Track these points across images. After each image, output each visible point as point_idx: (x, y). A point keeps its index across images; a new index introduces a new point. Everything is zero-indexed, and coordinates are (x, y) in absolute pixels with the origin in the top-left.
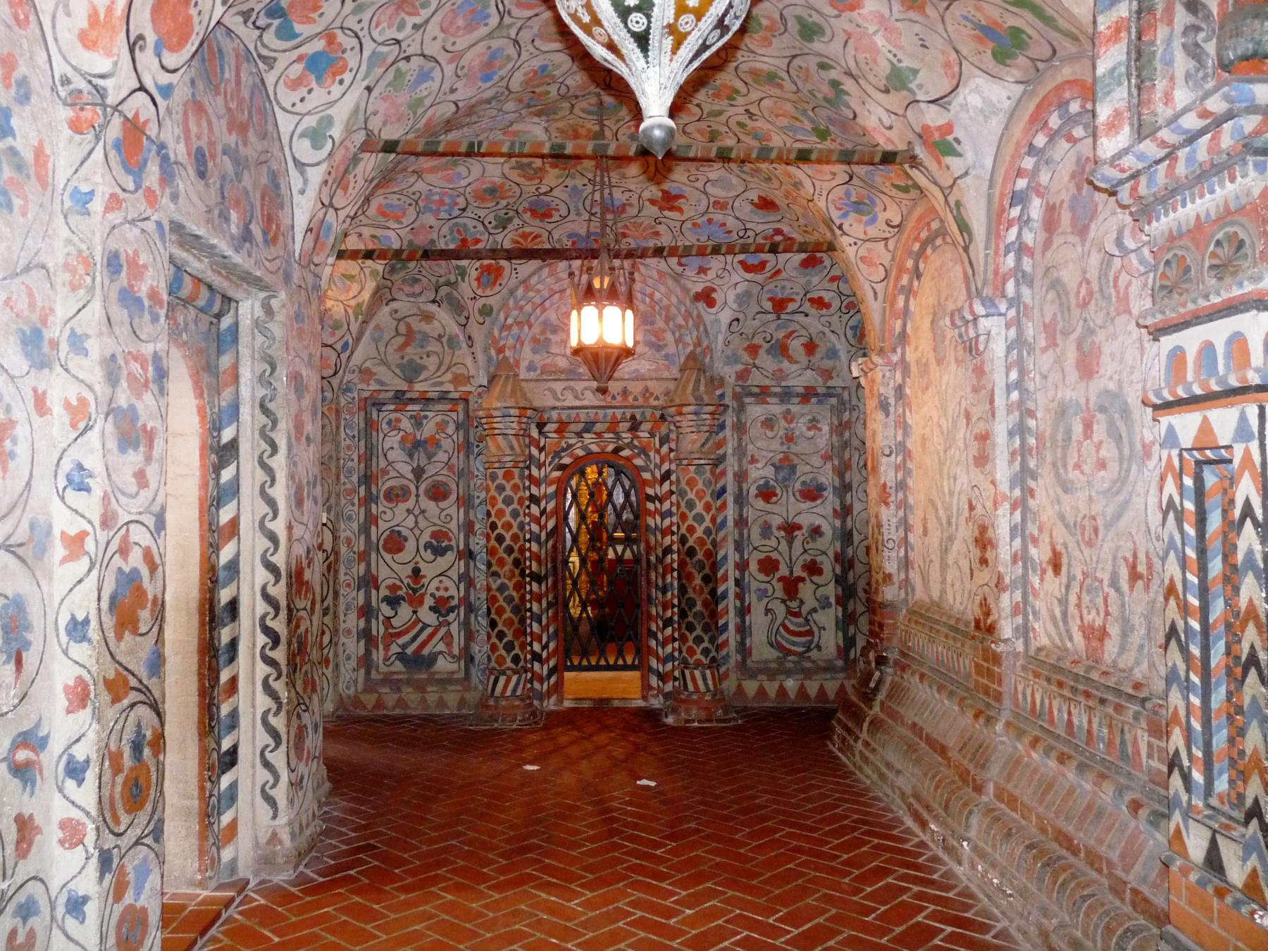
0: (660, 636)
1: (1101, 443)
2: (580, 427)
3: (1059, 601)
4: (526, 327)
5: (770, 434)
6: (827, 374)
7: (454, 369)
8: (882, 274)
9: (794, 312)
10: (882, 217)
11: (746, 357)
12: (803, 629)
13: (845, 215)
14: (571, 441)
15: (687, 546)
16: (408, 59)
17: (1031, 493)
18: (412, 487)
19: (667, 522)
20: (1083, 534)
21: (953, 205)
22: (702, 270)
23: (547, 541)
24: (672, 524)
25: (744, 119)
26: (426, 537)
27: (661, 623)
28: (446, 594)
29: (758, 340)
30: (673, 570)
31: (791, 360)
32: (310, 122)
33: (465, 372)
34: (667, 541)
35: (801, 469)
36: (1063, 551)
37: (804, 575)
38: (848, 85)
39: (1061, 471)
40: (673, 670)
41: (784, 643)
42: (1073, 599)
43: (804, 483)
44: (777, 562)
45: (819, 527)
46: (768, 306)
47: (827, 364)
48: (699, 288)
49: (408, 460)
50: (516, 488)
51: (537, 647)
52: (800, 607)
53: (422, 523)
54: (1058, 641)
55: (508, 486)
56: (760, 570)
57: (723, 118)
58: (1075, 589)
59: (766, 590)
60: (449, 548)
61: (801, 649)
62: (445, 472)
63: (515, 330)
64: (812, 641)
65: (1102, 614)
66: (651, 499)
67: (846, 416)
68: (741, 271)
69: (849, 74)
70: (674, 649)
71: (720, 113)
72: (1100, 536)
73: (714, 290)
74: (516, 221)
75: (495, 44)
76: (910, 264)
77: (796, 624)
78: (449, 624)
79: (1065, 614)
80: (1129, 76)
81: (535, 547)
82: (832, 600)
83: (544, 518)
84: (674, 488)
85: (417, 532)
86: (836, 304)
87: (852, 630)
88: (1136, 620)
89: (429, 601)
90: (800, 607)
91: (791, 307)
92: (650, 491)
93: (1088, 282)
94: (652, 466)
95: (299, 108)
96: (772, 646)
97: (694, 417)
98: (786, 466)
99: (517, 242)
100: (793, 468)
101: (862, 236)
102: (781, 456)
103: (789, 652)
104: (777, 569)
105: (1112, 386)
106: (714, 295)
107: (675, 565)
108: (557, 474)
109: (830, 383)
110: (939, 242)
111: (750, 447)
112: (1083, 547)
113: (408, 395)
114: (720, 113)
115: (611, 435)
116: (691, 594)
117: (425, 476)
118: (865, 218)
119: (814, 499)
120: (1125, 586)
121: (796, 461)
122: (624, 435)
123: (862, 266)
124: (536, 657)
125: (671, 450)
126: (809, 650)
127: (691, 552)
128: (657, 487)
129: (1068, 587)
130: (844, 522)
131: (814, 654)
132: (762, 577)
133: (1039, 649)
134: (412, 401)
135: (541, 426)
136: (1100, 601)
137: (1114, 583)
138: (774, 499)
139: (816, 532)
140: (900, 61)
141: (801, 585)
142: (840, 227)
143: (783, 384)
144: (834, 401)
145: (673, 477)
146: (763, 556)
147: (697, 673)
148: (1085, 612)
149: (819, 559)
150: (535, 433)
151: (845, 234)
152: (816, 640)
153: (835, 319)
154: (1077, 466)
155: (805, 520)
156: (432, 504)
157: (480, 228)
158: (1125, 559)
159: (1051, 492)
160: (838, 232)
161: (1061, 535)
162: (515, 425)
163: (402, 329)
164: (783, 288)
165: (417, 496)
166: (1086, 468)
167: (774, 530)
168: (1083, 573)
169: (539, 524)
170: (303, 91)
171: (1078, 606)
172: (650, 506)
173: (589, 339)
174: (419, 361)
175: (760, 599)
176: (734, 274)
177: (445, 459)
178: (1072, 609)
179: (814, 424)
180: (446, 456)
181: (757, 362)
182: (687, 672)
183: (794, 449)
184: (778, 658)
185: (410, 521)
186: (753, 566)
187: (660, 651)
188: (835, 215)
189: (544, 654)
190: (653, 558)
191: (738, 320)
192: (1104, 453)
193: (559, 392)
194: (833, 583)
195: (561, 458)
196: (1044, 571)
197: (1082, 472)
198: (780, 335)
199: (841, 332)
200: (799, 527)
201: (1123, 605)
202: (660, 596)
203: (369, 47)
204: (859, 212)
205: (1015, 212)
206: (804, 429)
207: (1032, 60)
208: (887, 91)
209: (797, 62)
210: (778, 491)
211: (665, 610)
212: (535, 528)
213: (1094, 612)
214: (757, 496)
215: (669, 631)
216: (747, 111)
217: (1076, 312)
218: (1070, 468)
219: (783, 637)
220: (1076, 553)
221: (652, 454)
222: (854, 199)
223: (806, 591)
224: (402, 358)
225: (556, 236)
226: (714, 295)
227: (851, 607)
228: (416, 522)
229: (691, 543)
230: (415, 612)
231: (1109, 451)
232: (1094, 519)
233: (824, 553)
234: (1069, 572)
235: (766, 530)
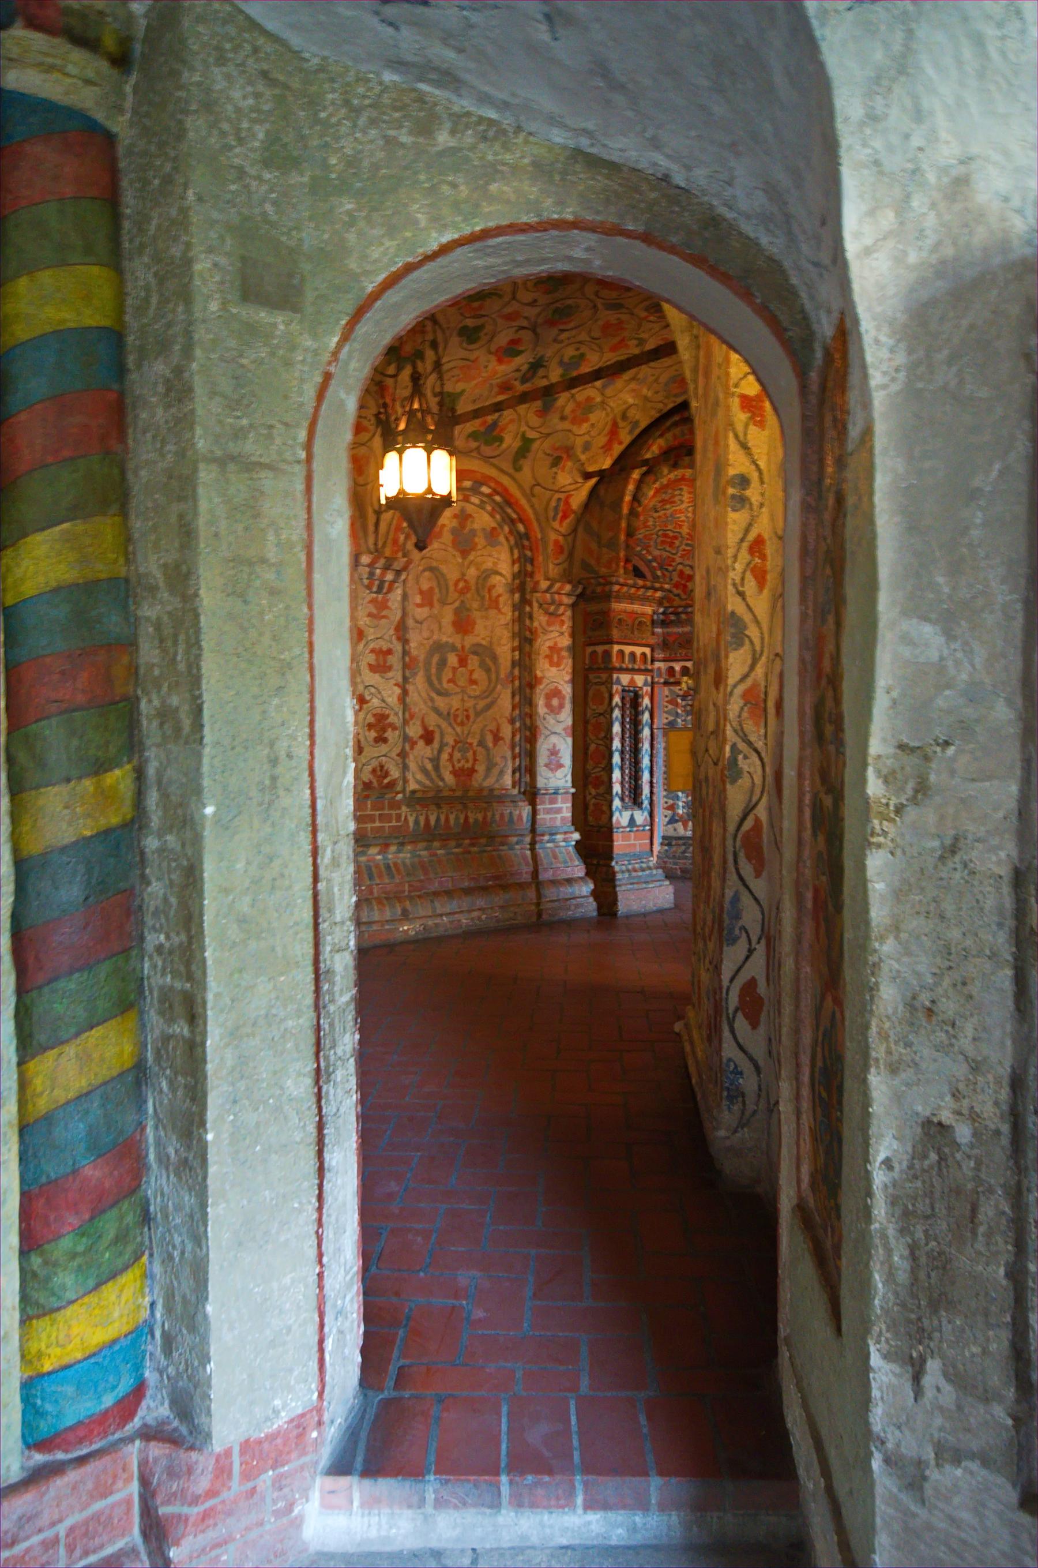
3: (431, 760)
39: (436, 682)
54: (428, 783)
79: (437, 768)
88: (498, 759)
120: (490, 745)
129: (440, 751)
133: (414, 792)
136: (470, 755)
159: (424, 694)
192: (475, 676)
196: (415, 743)
213: (463, 762)
220: (450, 730)
231: (479, 675)
234: (441, 741)
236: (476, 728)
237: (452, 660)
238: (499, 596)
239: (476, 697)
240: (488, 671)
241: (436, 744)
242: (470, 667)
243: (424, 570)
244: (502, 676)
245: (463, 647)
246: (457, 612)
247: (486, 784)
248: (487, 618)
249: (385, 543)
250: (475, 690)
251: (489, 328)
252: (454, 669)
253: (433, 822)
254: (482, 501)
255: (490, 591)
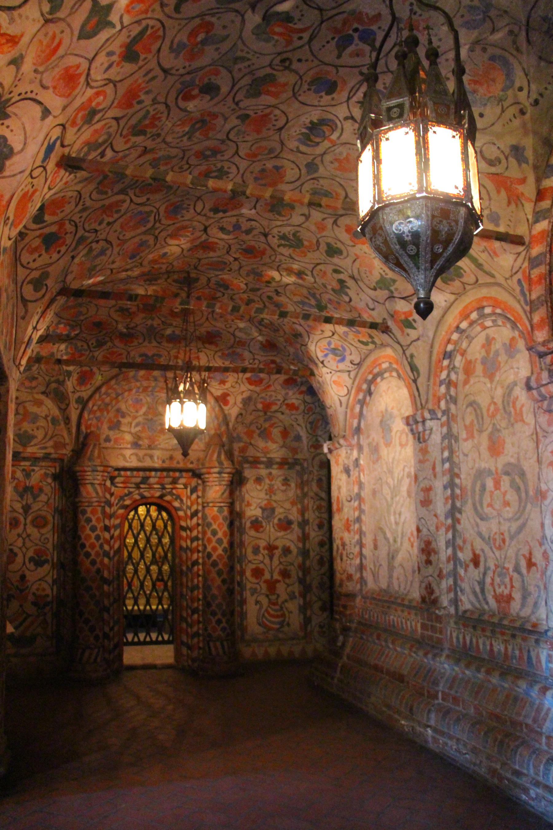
0: (189, 620)
1: (506, 492)
2: (138, 480)
3: (479, 583)
4: (105, 413)
5: (258, 487)
6: (294, 451)
7: (55, 439)
8: (346, 392)
9: (276, 411)
10: (348, 358)
11: (245, 438)
12: (279, 613)
13: (326, 355)
14: (131, 490)
15: (212, 559)
16: (97, 242)
17: (459, 521)
18: (22, 519)
19: (195, 544)
20: (494, 544)
21: (408, 355)
22: (223, 382)
23: (114, 556)
24: (198, 545)
25: (273, 295)
26: (30, 554)
27: (189, 611)
28: (43, 594)
29: (253, 428)
30: (199, 576)
31: (274, 442)
32: (36, 274)
33: (63, 441)
34: (195, 556)
35: (279, 510)
36: (481, 553)
37: (280, 578)
38: (350, 283)
39: (479, 508)
40: (198, 642)
41: (268, 623)
42: (488, 580)
43: (280, 520)
44: (263, 570)
45: (289, 547)
46: (260, 406)
47: (295, 444)
48: (218, 393)
49: (19, 499)
50: (98, 520)
51: (107, 629)
52: (277, 599)
53: (28, 544)
55: (94, 519)
56: (252, 576)
57: (259, 293)
58: (490, 574)
59: (256, 589)
60: (46, 561)
61: (277, 626)
62: (45, 508)
63: (98, 414)
64: (284, 621)
65: (509, 586)
66: (183, 528)
67: (305, 477)
68: (247, 385)
69: (353, 277)
70: (199, 629)
71: (258, 289)
72: (507, 543)
73: (228, 395)
74: (109, 344)
75: (144, 238)
76: (365, 386)
77: (276, 611)
78: (45, 614)
79: (483, 590)
80: (546, 302)
81: (106, 560)
82: (297, 594)
83: (112, 541)
84: (200, 522)
85: (24, 550)
86: (302, 407)
87: (309, 613)
88: (532, 589)
89: (31, 598)
90: (277, 599)
91: (274, 408)
92: (183, 524)
93: (495, 404)
94: (185, 507)
95: (33, 265)
96: (259, 624)
97: (217, 475)
98: (268, 510)
99: (107, 358)
100: (273, 510)
101: (335, 368)
102: (266, 502)
103: (270, 629)
104: (263, 575)
105: (512, 460)
106: (228, 398)
107: (201, 573)
108: (121, 511)
109: (296, 457)
110: (386, 375)
111: (247, 496)
112: (495, 550)
113: (22, 455)
114: (258, 289)
115: (159, 486)
116: (215, 591)
117: (31, 511)
118: (338, 358)
119: (285, 529)
120: (524, 571)
121: (275, 505)
122: (167, 486)
123: (333, 386)
124: (106, 636)
125: (198, 497)
126: (282, 626)
127: (215, 564)
128: (189, 521)
129: (485, 574)
130: (304, 544)
131: (286, 629)
132: (253, 580)
133: (465, 612)
134: (25, 459)
135: (112, 479)
136: (507, 580)
137: (517, 569)
138: (261, 529)
139: (287, 551)
140: (386, 274)
141: (278, 585)
142: (322, 362)
143: (268, 456)
144: (298, 468)
145: (200, 515)
146: (254, 566)
147: (218, 644)
148: (497, 587)
149: (289, 568)
150: (108, 483)
151: (324, 366)
152: (287, 619)
153: (300, 418)
154: (490, 505)
155: (280, 543)
156: (35, 530)
157: (86, 347)
158: (524, 556)
159: (472, 521)
160: (321, 365)
161: (479, 544)
162: (99, 477)
163: (21, 411)
164: (271, 396)
165: (25, 525)
166: (497, 507)
167: (261, 549)
168: (495, 565)
169: (109, 545)
170: (36, 255)
171: (492, 584)
172: (184, 534)
173: (175, 425)
174: (31, 432)
175: (252, 595)
176: (242, 385)
177: (46, 500)
178: (488, 587)
179: (286, 482)
180: (46, 497)
181: (253, 442)
182: (211, 644)
183: (274, 498)
184: (264, 633)
185: (20, 543)
186: (248, 573)
187: (189, 630)
188: (320, 355)
189: (111, 634)
190: (184, 568)
191: (241, 414)
192: (508, 497)
193: (127, 456)
194: (297, 584)
195: (124, 500)
196: (467, 566)
197: (494, 509)
198: (267, 425)
199: (303, 425)
200: (276, 548)
201: (523, 581)
202: (189, 593)
203: (81, 233)
204: (336, 355)
205: (446, 363)
206: (280, 485)
207: (463, 283)
208: (375, 289)
209: (319, 267)
210: (264, 524)
211: (193, 602)
212: (106, 547)
213: (503, 587)
214: (250, 528)
215: (196, 616)
216: (276, 290)
217: (487, 420)
218: (485, 505)
219: (267, 619)
220: (491, 554)
221: (185, 499)
222: (333, 346)
223: (281, 588)
224: (20, 430)
225: (132, 354)
226: (228, 398)
227: (308, 599)
228: (24, 543)
229: (214, 557)
230: (21, 606)
231: (511, 496)
232: (502, 534)
233: (293, 564)
234: (485, 566)
235: (256, 550)
236: (511, 552)
237: (490, 484)
238: (523, 406)
239: (509, 520)
240: (518, 490)
241: (482, 568)
242: (503, 489)
243: (467, 407)
244: (531, 493)
245: (497, 469)
246: (490, 438)
247: (522, 614)
248: (514, 434)
249: (427, 402)
250: (508, 512)
251: (329, 240)
252: (492, 493)
253: (468, 642)
254: (493, 321)
255: (514, 403)
